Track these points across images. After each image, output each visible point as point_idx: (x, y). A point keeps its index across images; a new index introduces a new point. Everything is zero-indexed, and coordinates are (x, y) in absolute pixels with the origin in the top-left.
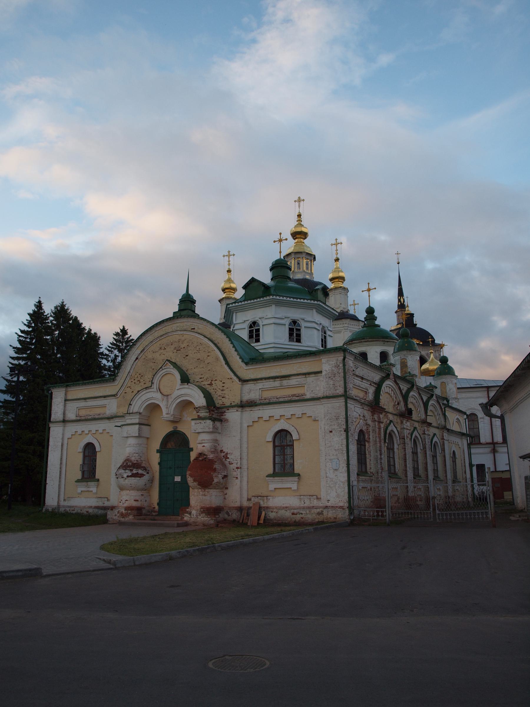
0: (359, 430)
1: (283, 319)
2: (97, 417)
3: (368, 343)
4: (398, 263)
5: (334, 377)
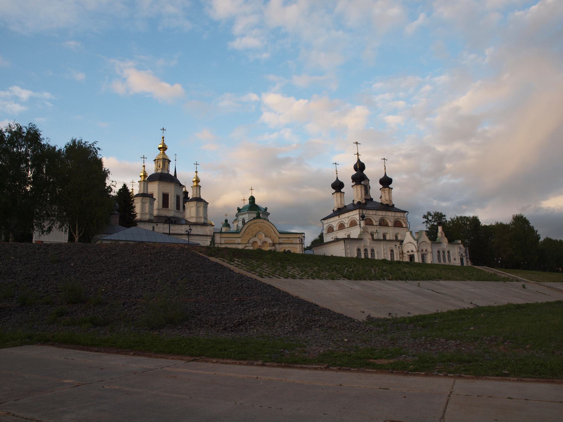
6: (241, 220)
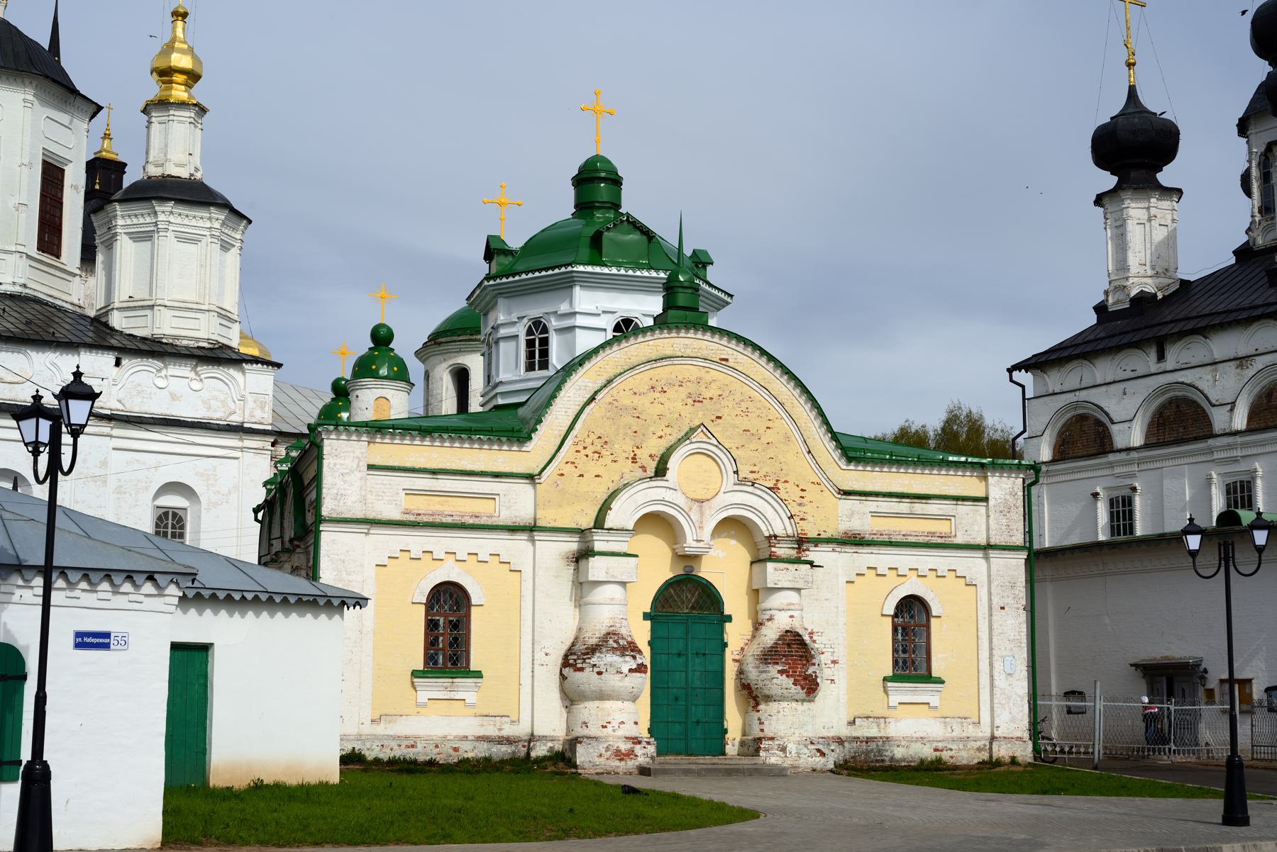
2: (471, 521)
5: (1009, 512)
6: (521, 330)
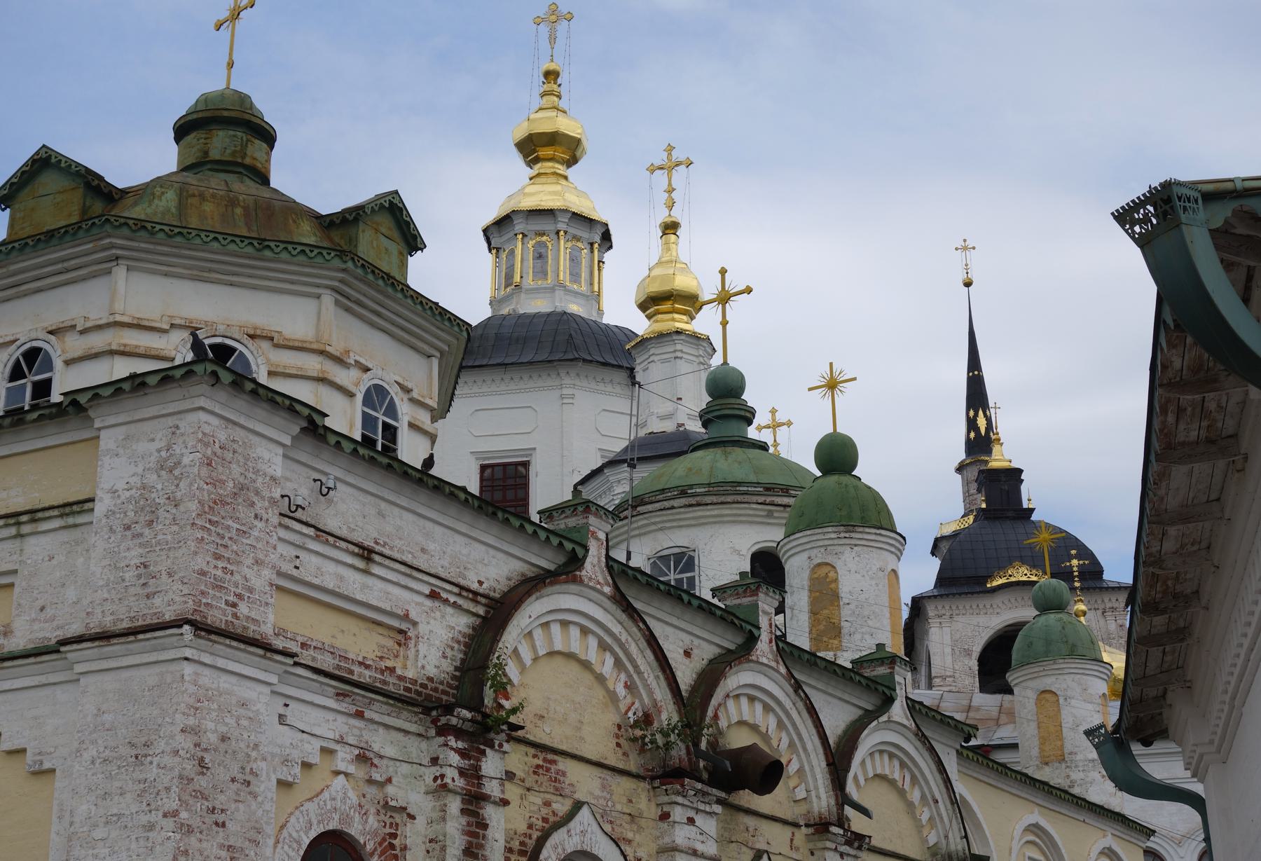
0: (313, 834)
1: (165, 331)
3: (699, 512)
4: (968, 284)
5: (150, 523)
